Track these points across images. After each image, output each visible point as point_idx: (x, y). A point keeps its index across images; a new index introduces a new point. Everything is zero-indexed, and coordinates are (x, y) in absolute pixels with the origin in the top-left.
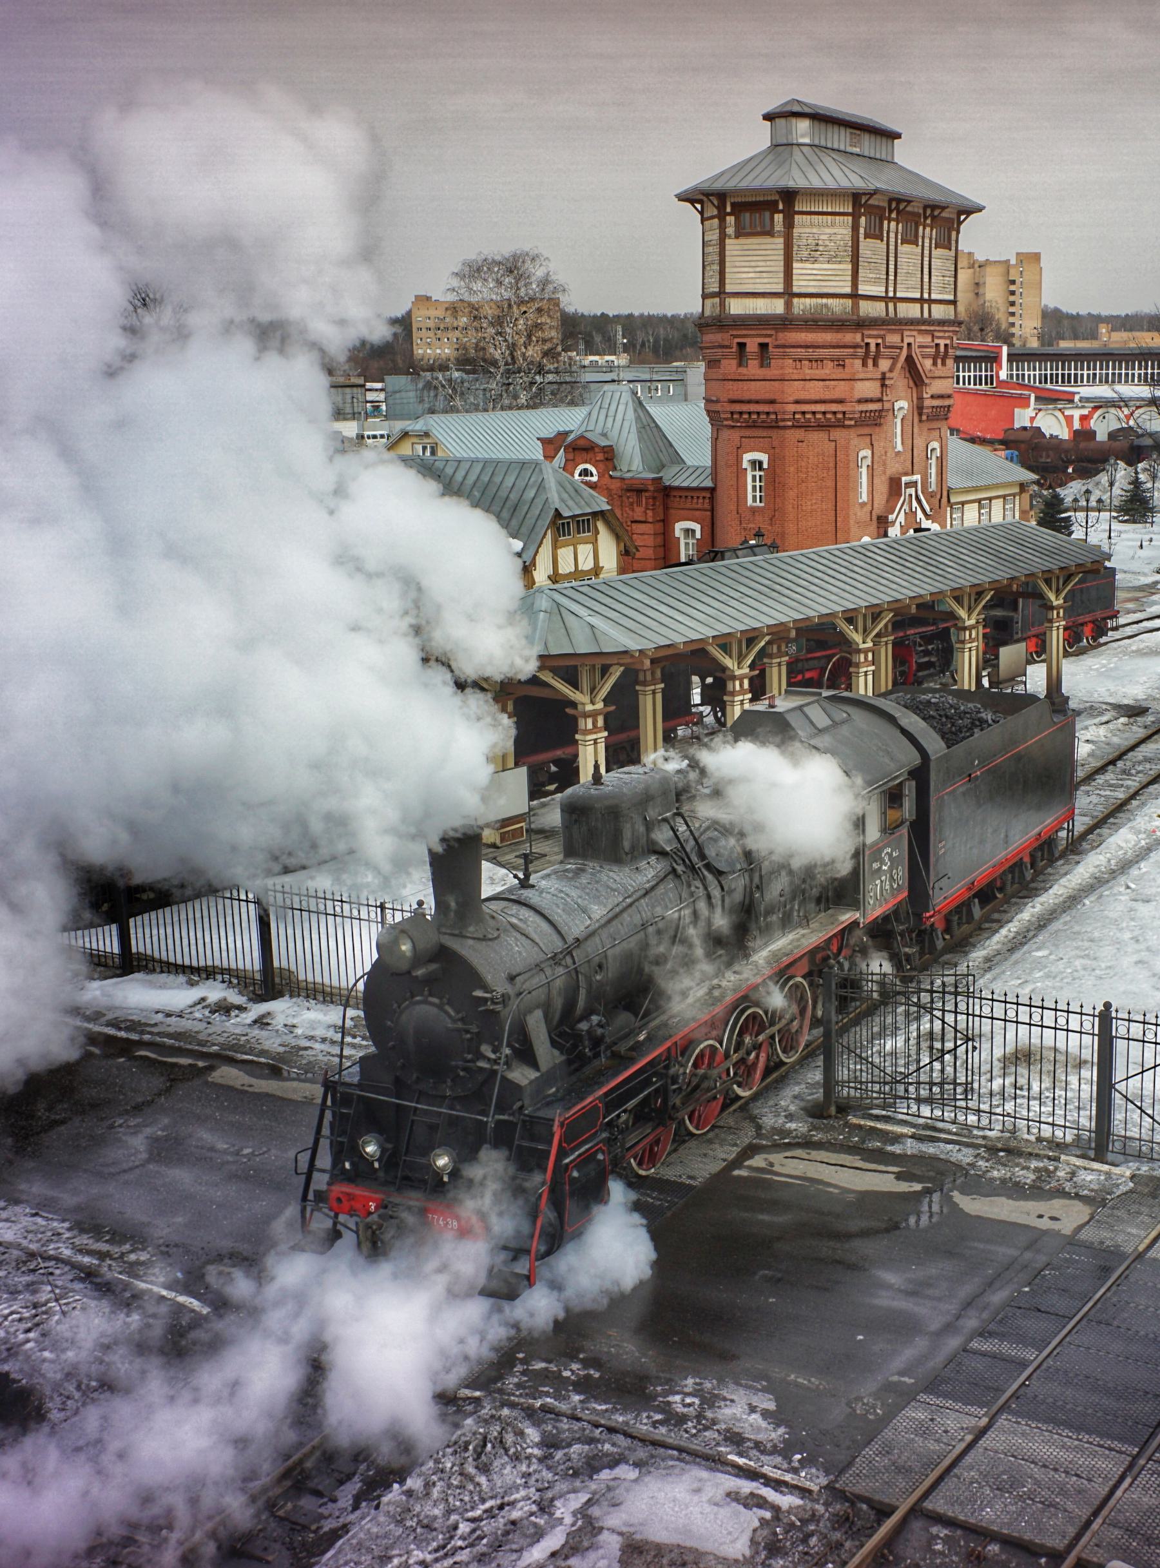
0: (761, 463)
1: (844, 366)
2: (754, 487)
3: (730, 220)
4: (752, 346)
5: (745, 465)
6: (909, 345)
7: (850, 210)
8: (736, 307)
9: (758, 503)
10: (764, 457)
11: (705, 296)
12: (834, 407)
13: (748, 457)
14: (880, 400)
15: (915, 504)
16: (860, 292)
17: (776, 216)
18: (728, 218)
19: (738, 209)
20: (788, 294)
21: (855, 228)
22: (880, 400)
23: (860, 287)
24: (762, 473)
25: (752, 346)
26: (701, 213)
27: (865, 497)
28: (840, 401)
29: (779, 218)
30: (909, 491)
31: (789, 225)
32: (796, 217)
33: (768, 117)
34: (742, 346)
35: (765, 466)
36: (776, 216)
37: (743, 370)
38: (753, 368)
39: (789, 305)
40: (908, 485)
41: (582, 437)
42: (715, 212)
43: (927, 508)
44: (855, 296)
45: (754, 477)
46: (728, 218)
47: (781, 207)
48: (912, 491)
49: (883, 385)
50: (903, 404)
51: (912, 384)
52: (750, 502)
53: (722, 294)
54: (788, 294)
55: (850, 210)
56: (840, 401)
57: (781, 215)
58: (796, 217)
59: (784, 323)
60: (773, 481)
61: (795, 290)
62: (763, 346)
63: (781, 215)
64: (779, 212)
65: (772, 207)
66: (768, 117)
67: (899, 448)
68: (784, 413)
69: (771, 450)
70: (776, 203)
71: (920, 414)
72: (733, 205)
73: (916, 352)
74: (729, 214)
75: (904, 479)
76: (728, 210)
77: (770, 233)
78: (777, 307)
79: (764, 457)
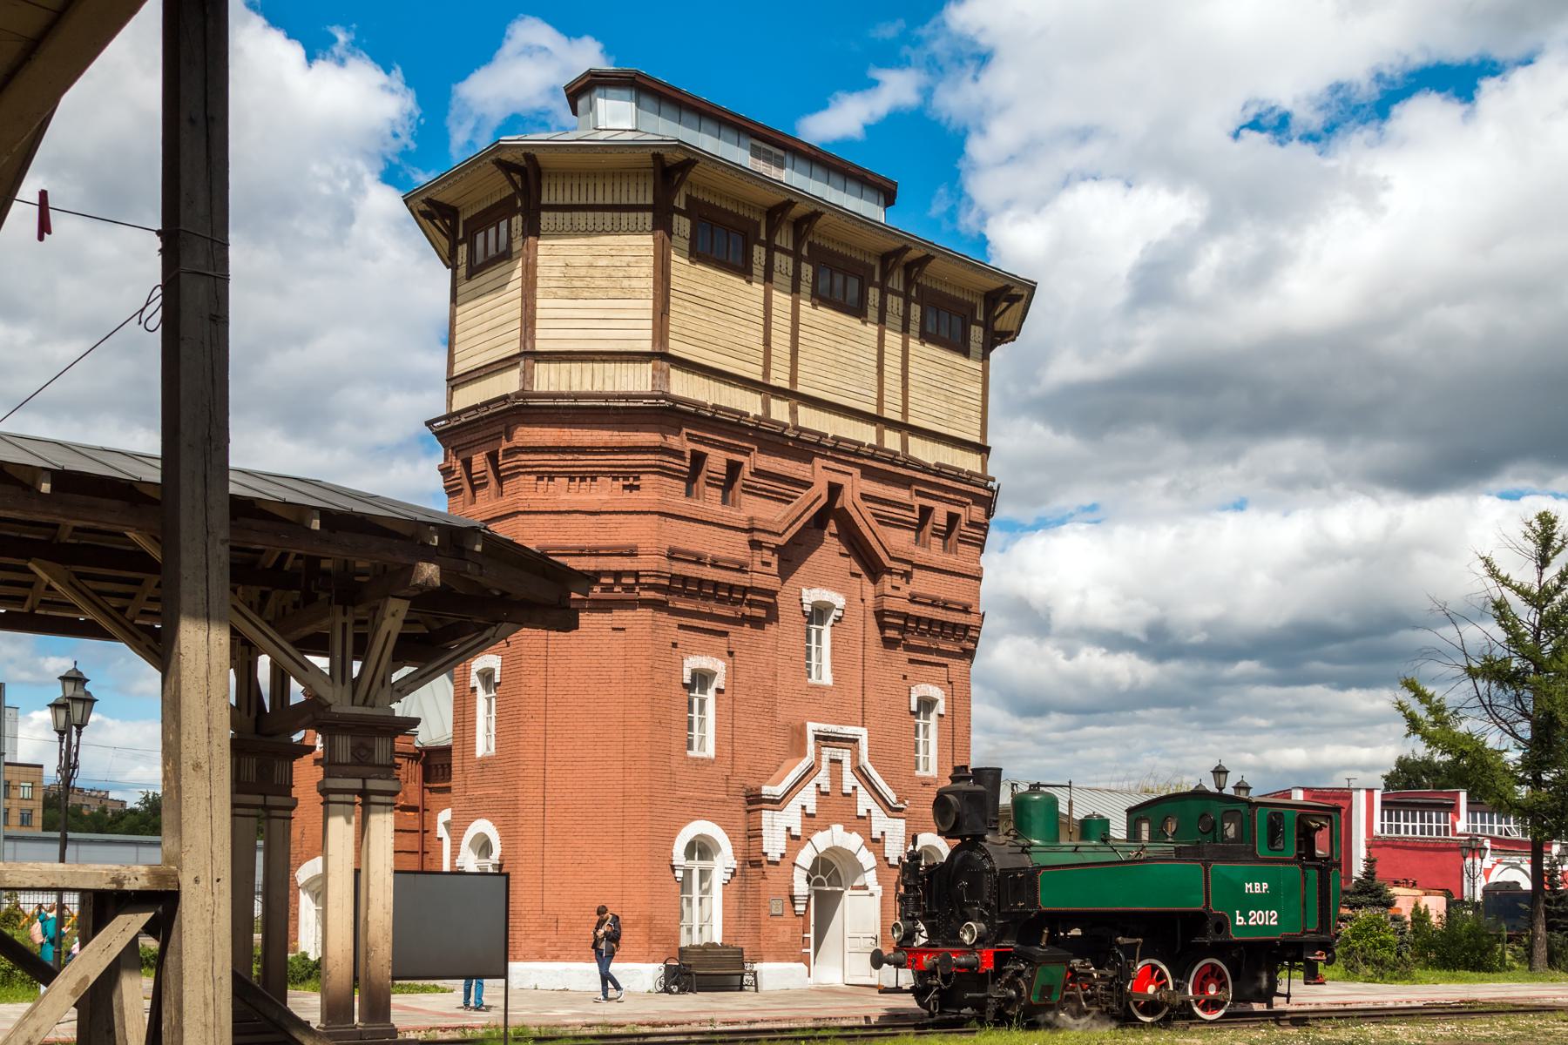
6: (835, 490)
12: (616, 564)
14: (741, 569)
15: (849, 781)
22: (741, 569)
28: (632, 553)
30: (827, 753)
32: (544, 215)
40: (823, 739)
43: (892, 797)
44: (660, 356)
48: (845, 756)
49: (755, 545)
56: (632, 553)
58: (544, 215)
67: (827, 679)
71: (883, 627)
73: (848, 500)
75: (812, 727)
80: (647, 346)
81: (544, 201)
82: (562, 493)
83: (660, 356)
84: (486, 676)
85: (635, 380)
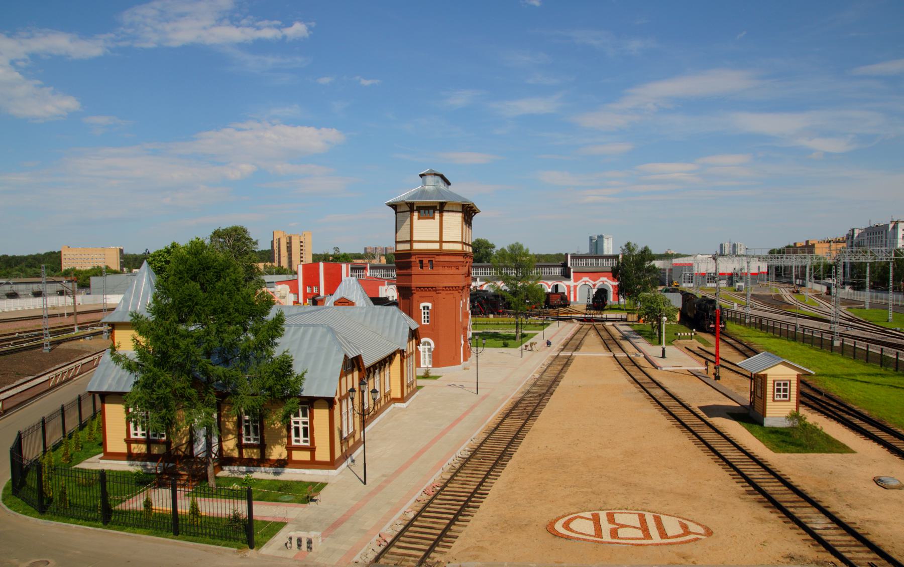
0: (428, 308)
5: (421, 308)
8: (416, 246)
10: (430, 305)
11: (397, 242)
13: (422, 305)
19: (419, 209)
20: (441, 241)
25: (425, 261)
31: (441, 217)
33: (421, 176)
34: (421, 262)
39: (441, 246)
42: (408, 209)
53: (411, 241)
54: (441, 241)
59: (440, 253)
77: (433, 218)
78: (436, 246)
79: (430, 305)
85: (458, 247)
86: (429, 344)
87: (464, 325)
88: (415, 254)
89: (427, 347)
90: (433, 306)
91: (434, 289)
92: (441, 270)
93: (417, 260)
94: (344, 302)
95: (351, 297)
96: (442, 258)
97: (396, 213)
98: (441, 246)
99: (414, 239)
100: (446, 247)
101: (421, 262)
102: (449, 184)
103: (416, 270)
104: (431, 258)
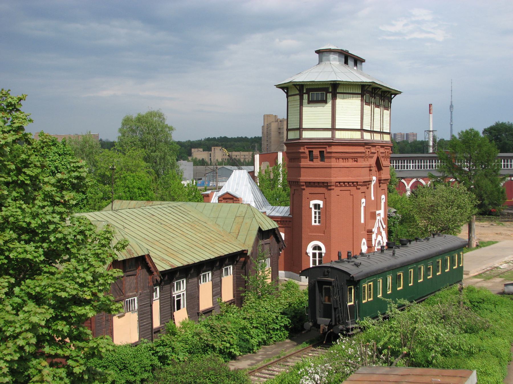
0: (319, 205)
1: (357, 161)
2: (315, 217)
3: (305, 96)
4: (316, 152)
5: (311, 206)
7: (360, 92)
8: (306, 135)
9: (317, 224)
10: (321, 203)
11: (288, 130)
13: (313, 202)
16: (364, 128)
17: (328, 94)
18: (304, 95)
20: (333, 129)
21: (362, 101)
23: (364, 126)
24: (319, 211)
25: (316, 152)
26: (287, 93)
27: (362, 221)
29: (329, 95)
31: (334, 98)
33: (318, 52)
34: (311, 152)
35: (321, 206)
36: (328, 94)
37: (311, 163)
38: (317, 163)
41: (228, 193)
42: (298, 92)
44: (362, 130)
45: (315, 213)
46: (304, 95)
47: (330, 90)
50: (374, 178)
51: (377, 170)
52: (313, 224)
53: (300, 129)
55: (360, 92)
57: (331, 94)
60: (324, 214)
61: (337, 127)
62: (321, 153)
63: (331, 94)
64: (330, 93)
65: (326, 90)
66: (318, 52)
67: (373, 198)
68: (331, 183)
69: (325, 200)
70: (328, 88)
71: (380, 183)
72: (307, 89)
74: (305, 93)
76: (305, 92)
77: (325, 102)
78: (328, 135)
79: (321, 203)
80: (359, 128)
81: (338, 91)
82: (342, 163)
83: (362, 130)
84: (317, 206)
85: (357, 136)
86: (319, 248)
87: (369, 228)
88: (303, 144)
89: (317, 252)
90: (325, 204)
91: (326, 185)
92: (334, 163)
93: (307, 151)
94: (229, 198)
95: (237, 194)
96: (334, 149)
97: (287, 97)
98: (333, 135)
99: (304, 126)
100: (339, 135)
101: (311, 152)
102: (358, 61)
103: (305, 162)
104: (322, 149)
